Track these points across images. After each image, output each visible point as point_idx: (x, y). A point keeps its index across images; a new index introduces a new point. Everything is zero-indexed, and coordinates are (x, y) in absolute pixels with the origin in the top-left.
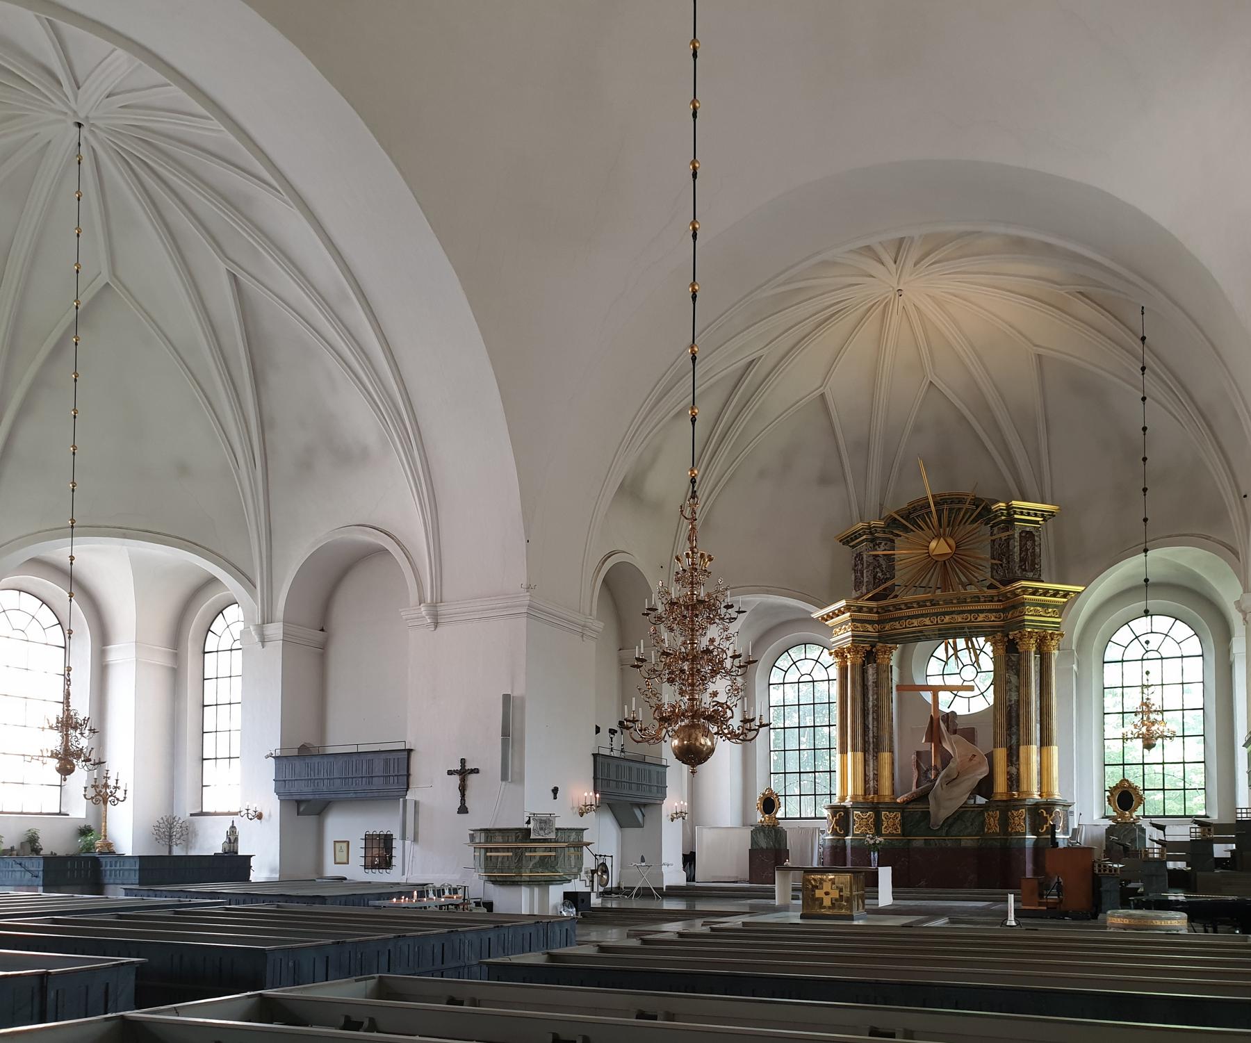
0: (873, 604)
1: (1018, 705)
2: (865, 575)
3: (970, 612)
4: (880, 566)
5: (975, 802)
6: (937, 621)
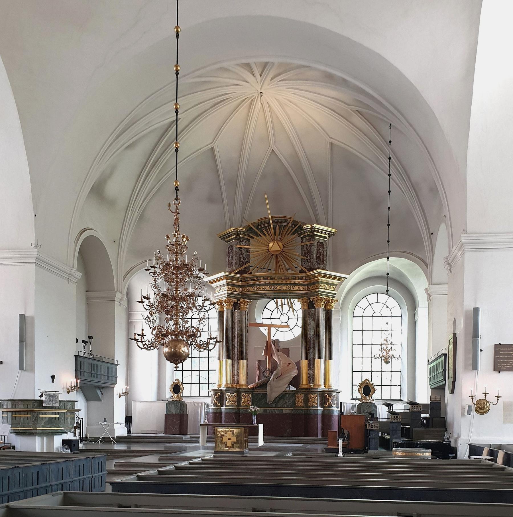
4: (242, 254)
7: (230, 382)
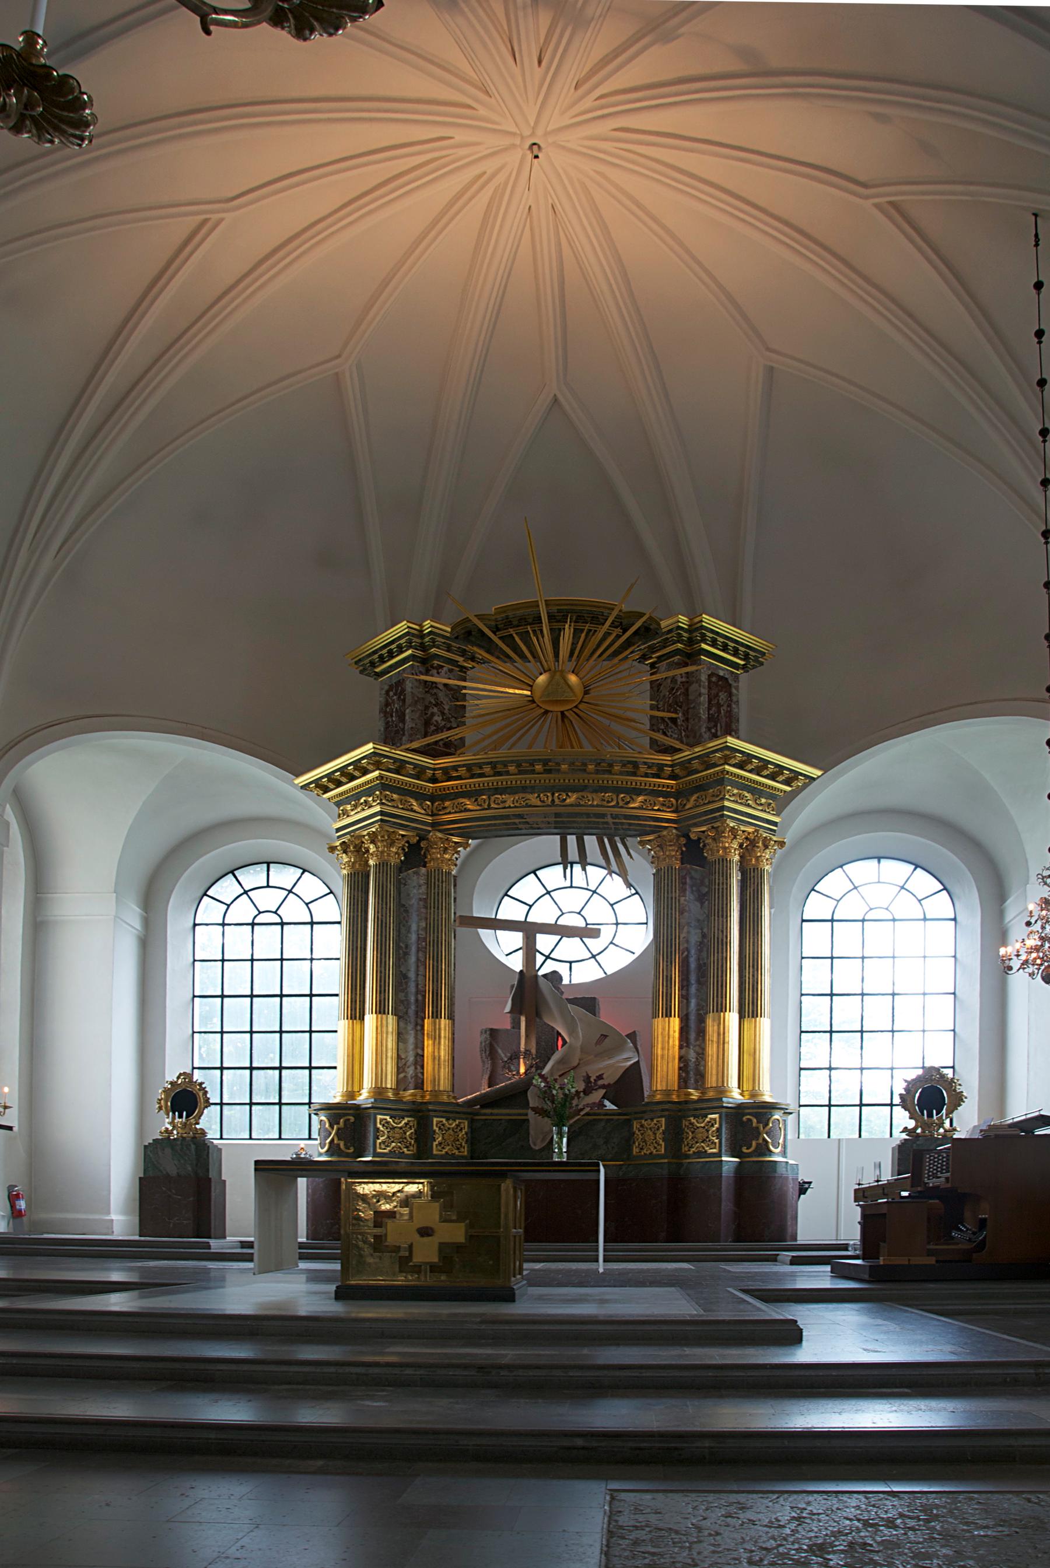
7: (390, 1083)
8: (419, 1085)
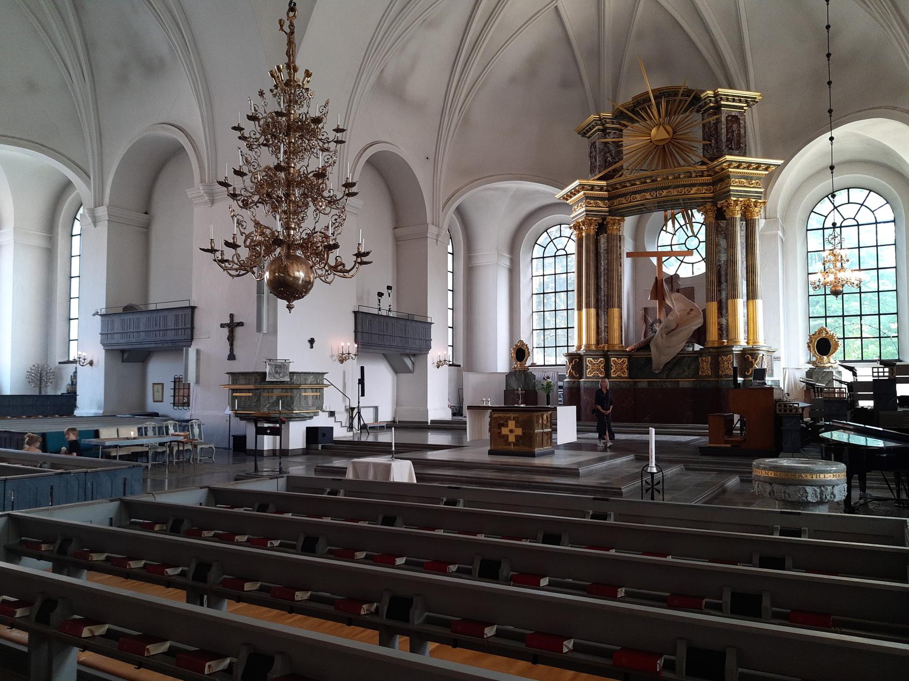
0: (603, 183)
1: (727, 265)
2: (597, 161)
3: (684, 186)
5: (693, 349)
6: (656, 195)
8: (607, 342)
